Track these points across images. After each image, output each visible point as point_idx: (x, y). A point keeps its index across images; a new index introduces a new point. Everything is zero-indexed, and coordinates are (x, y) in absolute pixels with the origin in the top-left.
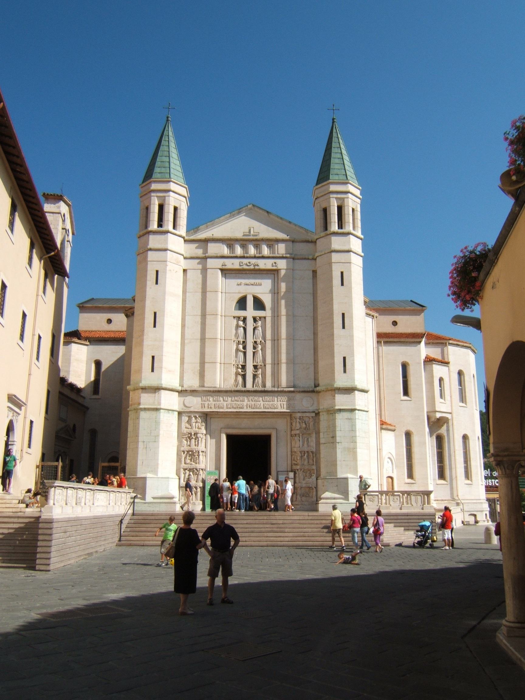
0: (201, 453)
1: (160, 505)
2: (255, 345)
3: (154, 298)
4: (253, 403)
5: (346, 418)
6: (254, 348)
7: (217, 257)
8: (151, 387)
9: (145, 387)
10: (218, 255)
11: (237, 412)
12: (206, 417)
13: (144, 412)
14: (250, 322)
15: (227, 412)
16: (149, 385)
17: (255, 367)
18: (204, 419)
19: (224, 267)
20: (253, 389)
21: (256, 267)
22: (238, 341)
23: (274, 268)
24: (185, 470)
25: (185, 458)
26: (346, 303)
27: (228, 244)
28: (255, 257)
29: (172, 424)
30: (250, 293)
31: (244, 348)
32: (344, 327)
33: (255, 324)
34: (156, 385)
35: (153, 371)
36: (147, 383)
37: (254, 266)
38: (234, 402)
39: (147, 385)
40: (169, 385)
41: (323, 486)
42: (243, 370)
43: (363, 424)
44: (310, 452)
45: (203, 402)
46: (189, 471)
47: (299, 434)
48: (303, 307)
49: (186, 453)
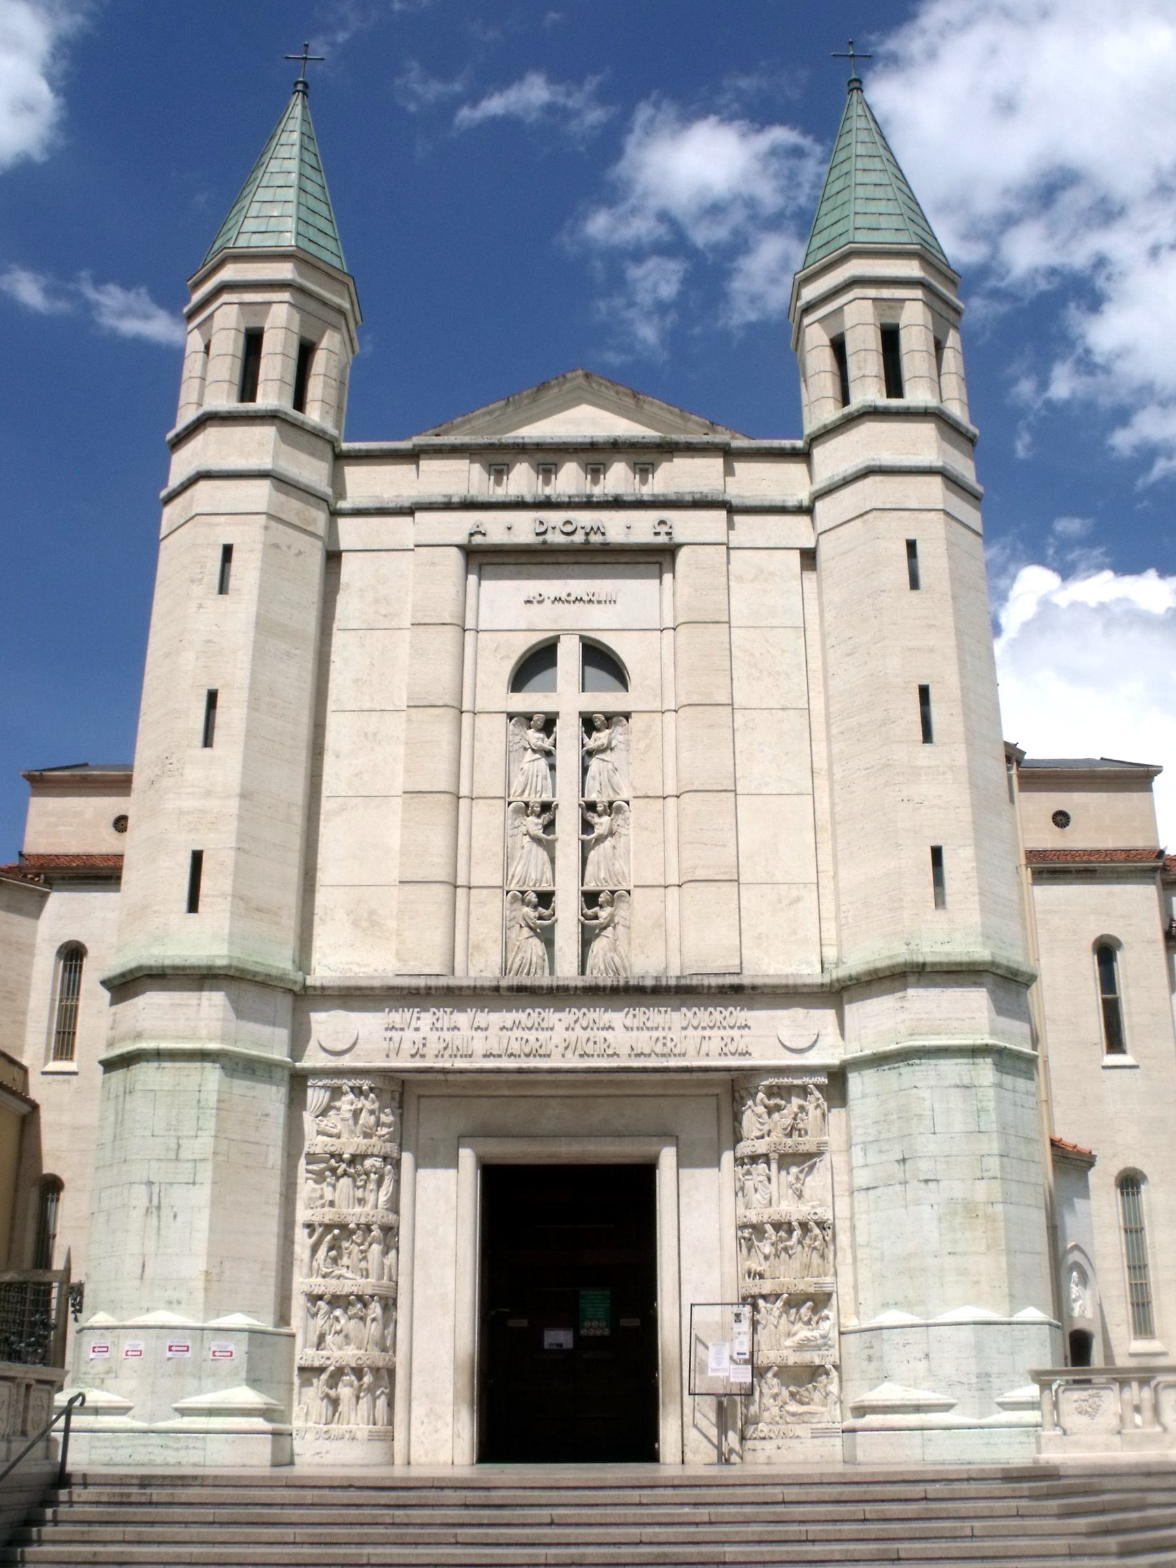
0: (376, 1232)
1: (204, 1439)
2: (594, 818)
3: (210, 641)
4: (585, 1035)
5: (953, 1082)
6: (587, 827)
7: (448, 506)
8: (184, 968)
9: (163, 968)
10: (455, 499)
11: (520, 1071)
12: (402, 1095)
13: (156, 1064)
14: (568, 731)
15: (481, 1071)
16: (178, 962)
17: (591, 898)
18: (393, 1098)
19: (478, 539)
20: (580, 982)
21: (595, 539)
22: (527, 804)
23: (663, 539)
24: (314, 1298)
25: (315, 1249)
26: (932, 650)
27: (490, 465)
28: (589, 504)
29: (267, 1115)
30: (570, 632)
31: (549, 827)
32: (927, 736)
33: (586, 739)
34: (204, 962)
35: (193, 906)
36: (169, 953)
37: (587, 534)
38: (509, 1033)
39: (167, 962)
40: (256, 963)
41: (870, 1359)
42: (545, 912)
43: (1020, 1108)
44: (812, 1223)
45: (389, 1034)
46: (329, 1303)
47: (766, 1155)
48: (770, 674)
49: (319, 1230)
